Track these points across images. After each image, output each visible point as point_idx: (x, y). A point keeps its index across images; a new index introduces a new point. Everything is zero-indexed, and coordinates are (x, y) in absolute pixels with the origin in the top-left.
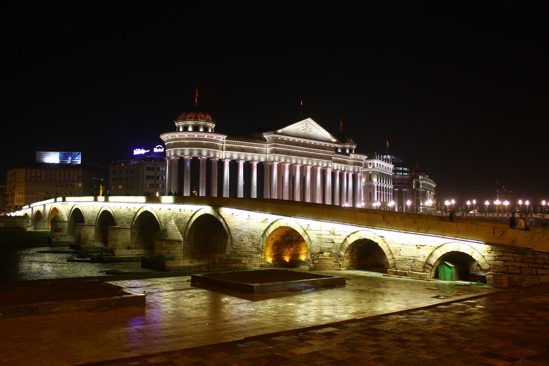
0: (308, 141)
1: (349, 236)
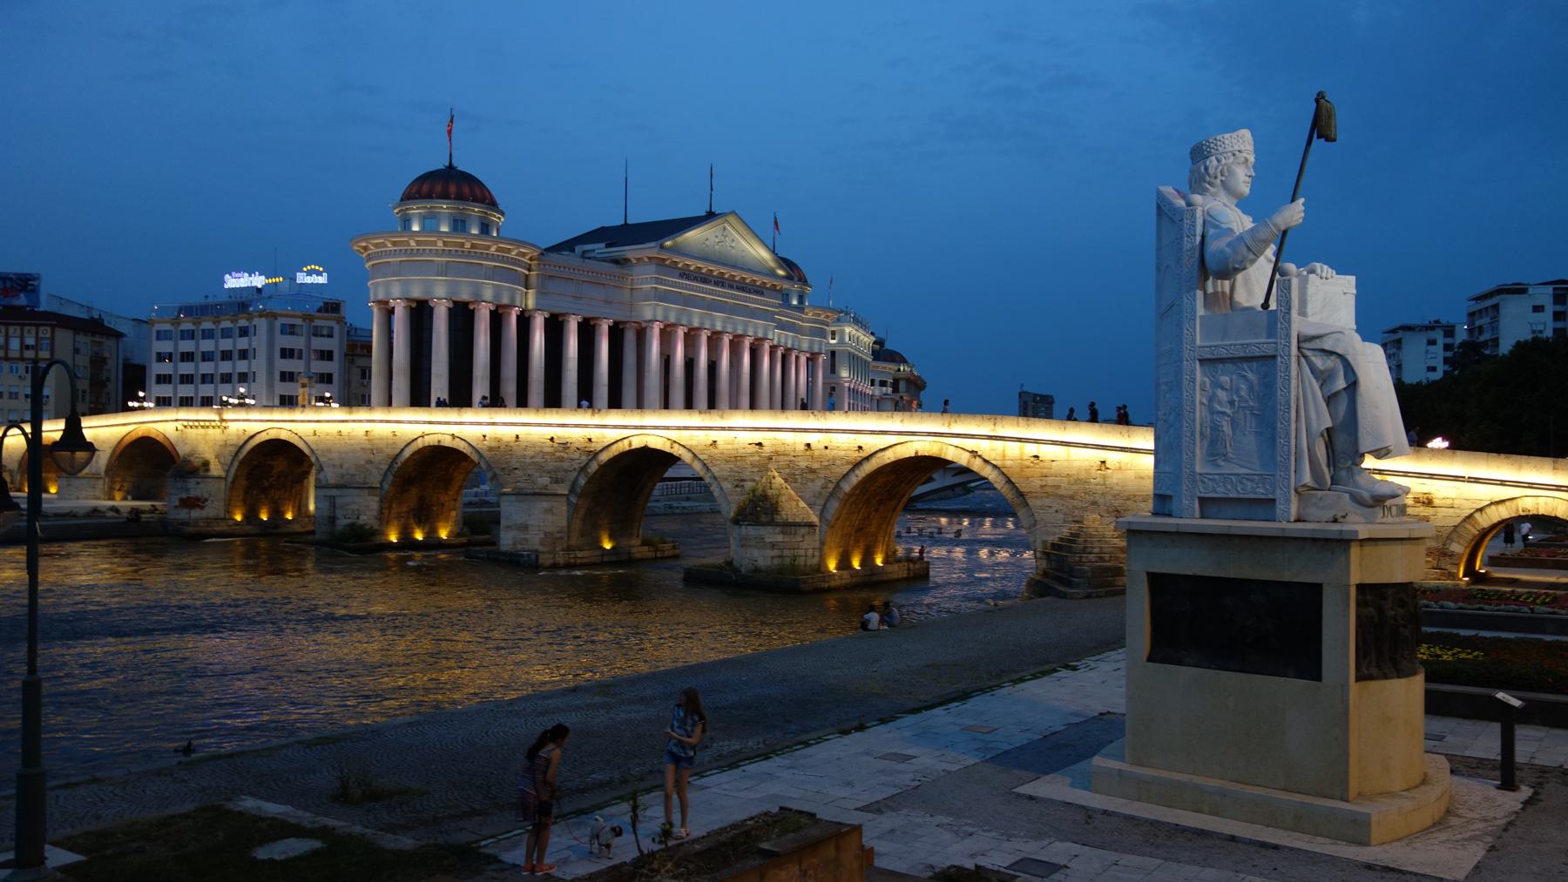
0: (728, 273)
1: (1481, 510)
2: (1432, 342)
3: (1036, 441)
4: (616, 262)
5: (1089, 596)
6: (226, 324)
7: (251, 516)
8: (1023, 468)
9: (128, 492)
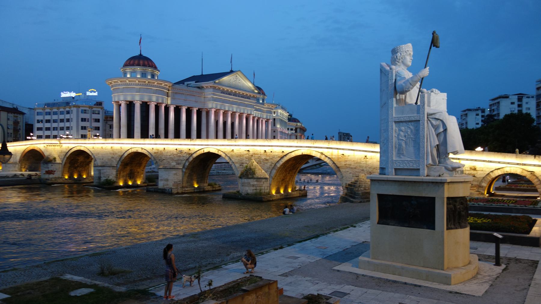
0: (238, 91)
1: (492, 172)
2: (477, 115)
3: (343, 149)
4: (199, 88)
5: (361, 202)
6: (62, 110)
7: (71, 177)
8: (338, 158)
9: (27, 169)
